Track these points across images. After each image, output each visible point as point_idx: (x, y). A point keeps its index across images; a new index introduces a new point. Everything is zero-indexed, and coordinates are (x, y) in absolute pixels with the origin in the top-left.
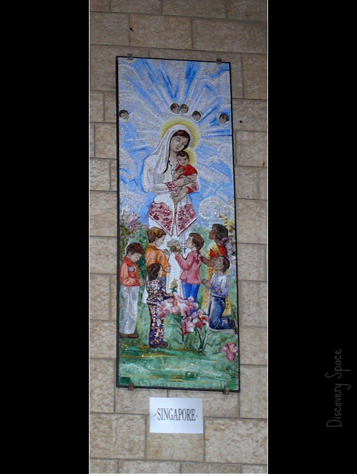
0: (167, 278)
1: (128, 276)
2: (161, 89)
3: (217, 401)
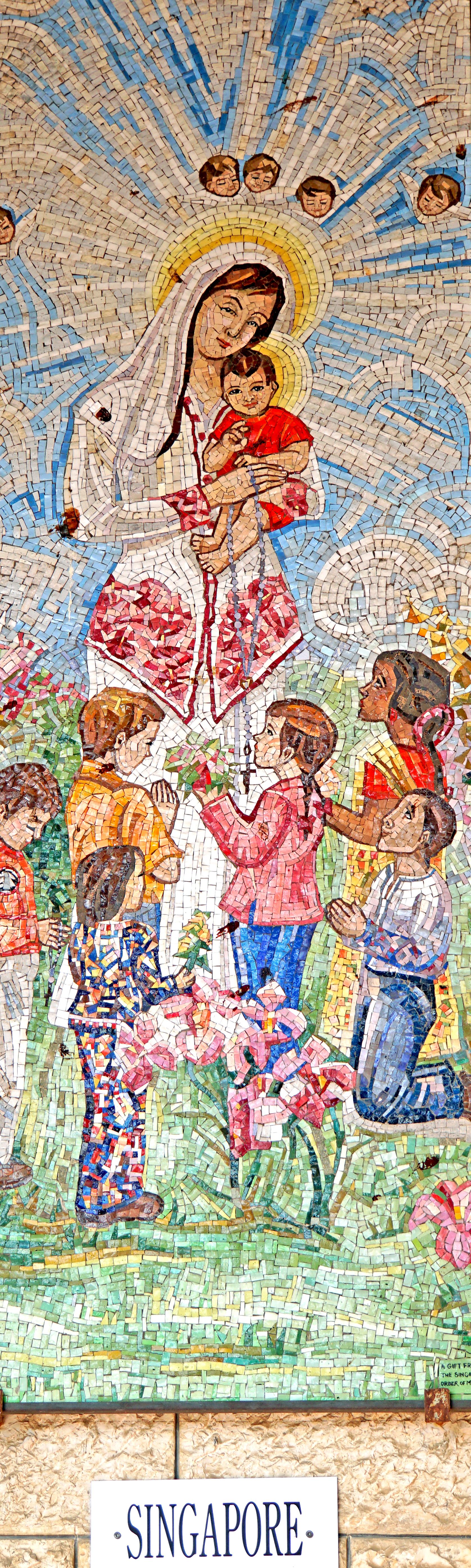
0: (165, 909)
2: (162, 100)
3: (413, 1456)
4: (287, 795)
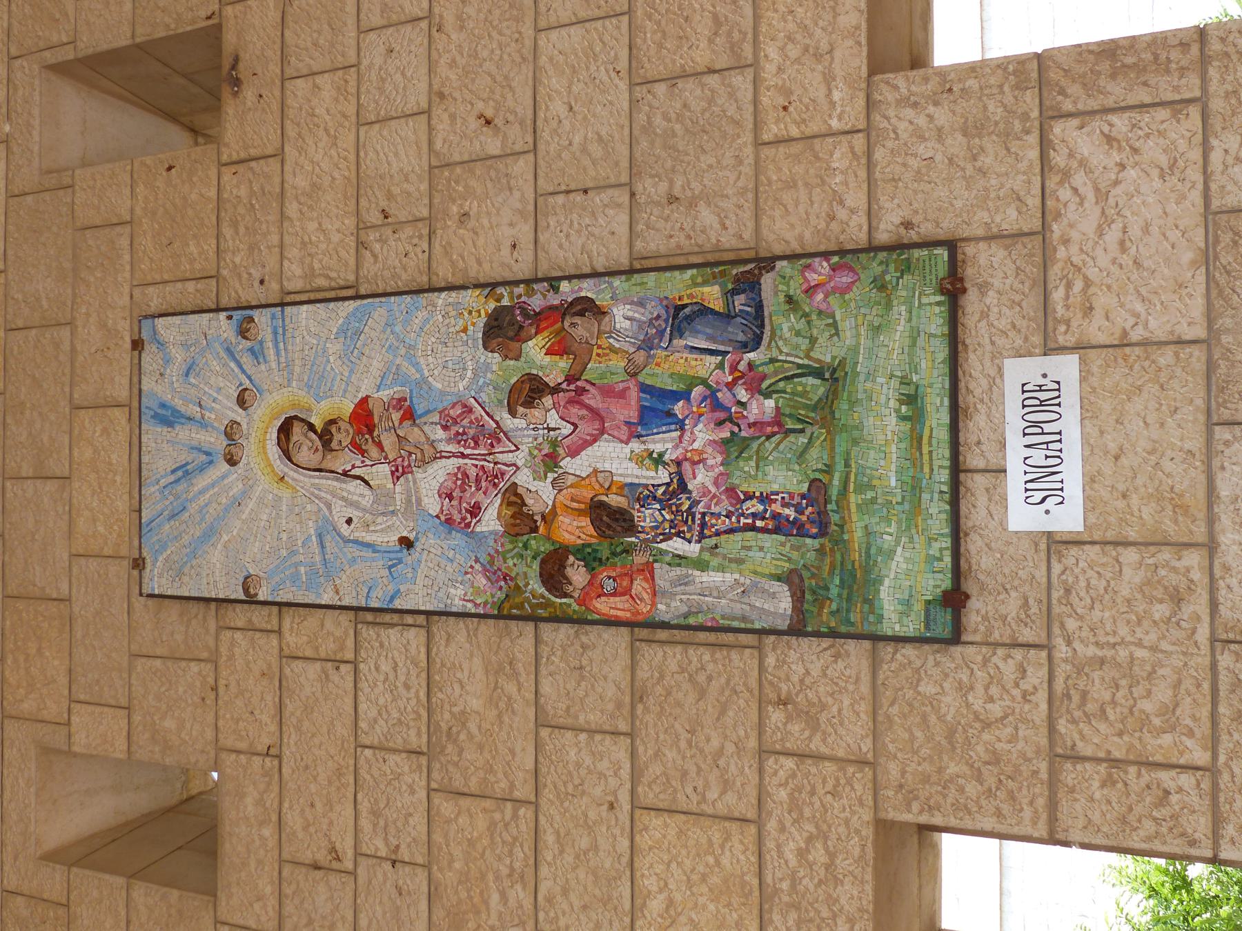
0: (629, 480)
1: (627, 597)
3: (989, 308)
4: (562, 404)
